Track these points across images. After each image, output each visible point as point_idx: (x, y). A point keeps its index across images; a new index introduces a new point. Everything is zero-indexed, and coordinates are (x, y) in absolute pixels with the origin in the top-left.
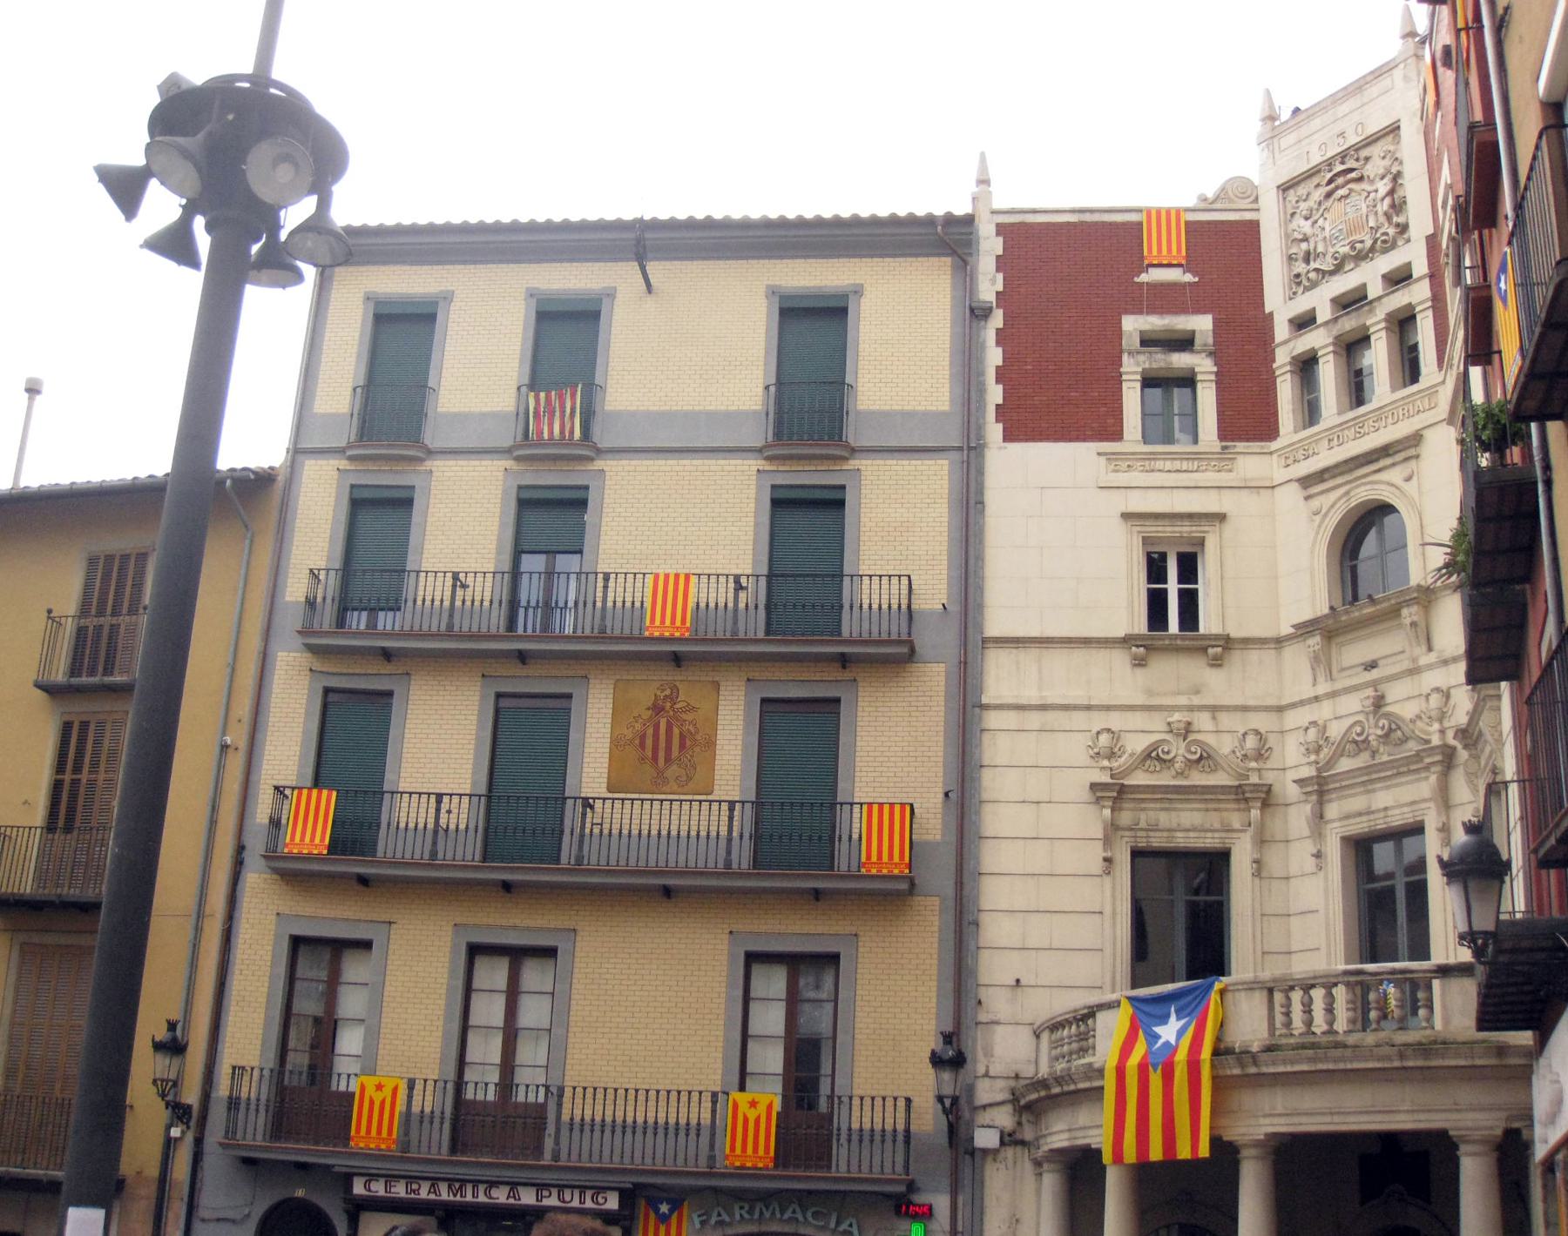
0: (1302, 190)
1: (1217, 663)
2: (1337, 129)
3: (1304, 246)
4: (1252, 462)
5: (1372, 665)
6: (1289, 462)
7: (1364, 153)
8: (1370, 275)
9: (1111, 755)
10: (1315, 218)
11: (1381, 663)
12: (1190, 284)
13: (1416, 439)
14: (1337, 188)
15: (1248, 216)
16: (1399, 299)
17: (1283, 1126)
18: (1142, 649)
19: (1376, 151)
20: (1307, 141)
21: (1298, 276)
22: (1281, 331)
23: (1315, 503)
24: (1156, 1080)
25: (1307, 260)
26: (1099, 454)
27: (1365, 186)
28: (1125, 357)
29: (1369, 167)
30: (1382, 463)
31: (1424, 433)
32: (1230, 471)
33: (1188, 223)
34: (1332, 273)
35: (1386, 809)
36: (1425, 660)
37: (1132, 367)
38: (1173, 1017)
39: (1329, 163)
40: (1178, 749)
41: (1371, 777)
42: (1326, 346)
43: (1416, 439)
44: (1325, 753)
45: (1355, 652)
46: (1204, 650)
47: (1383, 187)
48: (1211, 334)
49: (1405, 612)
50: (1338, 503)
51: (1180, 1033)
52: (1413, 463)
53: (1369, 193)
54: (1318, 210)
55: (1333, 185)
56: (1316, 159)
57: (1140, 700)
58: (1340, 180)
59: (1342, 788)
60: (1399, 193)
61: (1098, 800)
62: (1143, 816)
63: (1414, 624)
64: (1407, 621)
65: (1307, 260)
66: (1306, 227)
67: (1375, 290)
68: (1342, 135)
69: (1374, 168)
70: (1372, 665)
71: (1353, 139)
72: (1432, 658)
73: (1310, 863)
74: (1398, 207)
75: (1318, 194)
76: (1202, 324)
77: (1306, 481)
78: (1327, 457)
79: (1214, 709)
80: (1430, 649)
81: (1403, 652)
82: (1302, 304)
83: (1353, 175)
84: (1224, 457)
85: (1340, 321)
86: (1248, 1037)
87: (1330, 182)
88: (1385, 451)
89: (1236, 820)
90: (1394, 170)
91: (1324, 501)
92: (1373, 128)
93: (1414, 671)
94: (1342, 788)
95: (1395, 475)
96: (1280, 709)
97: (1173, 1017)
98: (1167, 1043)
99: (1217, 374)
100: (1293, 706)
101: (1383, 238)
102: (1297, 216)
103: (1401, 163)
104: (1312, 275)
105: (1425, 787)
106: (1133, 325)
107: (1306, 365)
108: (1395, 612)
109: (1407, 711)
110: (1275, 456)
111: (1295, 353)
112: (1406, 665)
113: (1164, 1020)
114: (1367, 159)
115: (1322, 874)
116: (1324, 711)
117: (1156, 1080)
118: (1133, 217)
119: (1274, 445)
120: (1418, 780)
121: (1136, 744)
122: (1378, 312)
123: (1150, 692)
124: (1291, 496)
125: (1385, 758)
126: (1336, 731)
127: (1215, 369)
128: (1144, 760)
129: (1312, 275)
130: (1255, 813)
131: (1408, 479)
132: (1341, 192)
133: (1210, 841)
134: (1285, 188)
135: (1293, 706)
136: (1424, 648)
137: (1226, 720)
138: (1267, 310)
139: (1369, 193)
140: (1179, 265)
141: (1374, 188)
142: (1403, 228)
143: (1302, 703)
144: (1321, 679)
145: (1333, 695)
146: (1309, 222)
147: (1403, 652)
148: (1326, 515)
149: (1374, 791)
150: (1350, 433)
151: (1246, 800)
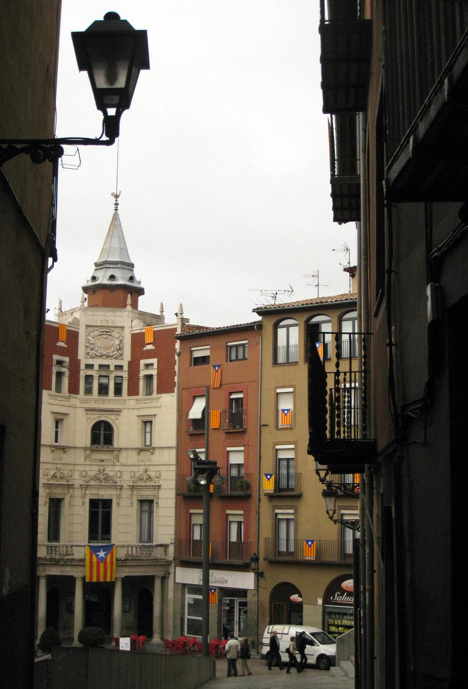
0: (91, 329)
1: (65, 452)
2: (107, 318)
3: (92, 346)
4: (76, 400)
5: (102, 461)
6: (83, 402)
7: (113, 329)
8: (112, 363)
9: (47, 475)
10: (95, 339)
11: (104, 461)
12: (65, 348)
13: (120, 411)
14: (103, 334)
15: (77, 330)
16: (119, 373)
17: (127, 574)
18: (54, 449)
19: (116, 330)
20: (96, 317)
21: (89, 353)
22: (82, 367)
23: (89, 416)
24: (102, 565)
25: (92, 349)
26: (48, 394)
27: (111, 337)
28: (53, 366)
29: (113, 333)
30: (109, 413)
31: (123, 411)
32: (69, 402)
33: (67, 329)
34: (99, 356)
35: (103, 495)
36: (117, 464)
37: (55, 369)
38: (102, 551)
39: (103, 327)
40: (58, 475)
41: (99, 487)
42: (96, 376)
43: (120, 411)
44: (87, 478)
45: (98, 456)
46: (64, 449)
47: (117, 342)
48: (68, 363)
49: (115, 452)
50: (95, 418)
51: (106, 555)
52: (118, 416)
53: (112, 340)
54: (96, 337)
55: (102, 333)
56: (99, 324)
57: (52, 461)
58: (105, 333)
59: (92, 488)
60: (121, 345)
61: (44, 487)
62: (51, 490)
63: (116, 455)
64: (115, 454)
65: (92, 349)
66: (92, 341)
67: (112, 368)
68: (107, 321)
69: (115, 334)
70: (102, 461)
71: (110, 324)
72: (119, 464)
73: (80, 504)
74: (121, 349)
75: (96, 333)
76: (67, 359)
77: (88, 410)
78: (92, 405)
79: (64, 464)
80: (118, 462)
81: (110, 460)
82: (90, 362)
83: (109, 334)
84: (69, 398)
85: (101, 371)
86: (120, 557)
87: (102, 332)
88: (112, 411)
89: (66, 491)
90: (121, 338)
91: (92, 417)
92: (118, 324)
93: (114, 465)
94: (92, 488)
95: (113, 417)
96: (75, 465)
97: (102, 551)
98: (102, 557)
99: (69, 375)
100: (78, 465)
101: (116, 355)
102: (89, 336)
103: (123, 337)
104: (94, 355)
105: (114, 492)
106: (56, 357)
107: (89, 378)
108: (113, 451)
109: (111, 474)
110: (78, 399)
111: (87, 374)
112: (112, 463)
113: (99, 551)
114: (113, 331)
115: (83, 507)
116: (88, 468)
117: (102, 565)
118: (57, 326)
119: (78, 396)
120: (112, 490)
121: (52, 473)
122: (112, 374)
123: (53, 459)
124: (81, 412)
125: (103, 484)
126: (92, 474)
127: (69, 373)
128: (52, 477)
129: (94, 355)
130: (71, 491)
131: (117, 419)
132: (105, 336)
133: (62, 497)
134: (87, 326)
135: (78, 465)
136: (117, 460)
137: (66, 467)
138: (79, 358)
139: (112, 340)
140: (65, 342)
141: (114, 339)
142: (121, 355)
143: (81, 465)
144: (87, 460)
145: (90, 465)
146: (93, 339)
147: (110, 460)
148: (92, 420)
149: (100, 490)
150: (101, 402)
151: (69, 487)
